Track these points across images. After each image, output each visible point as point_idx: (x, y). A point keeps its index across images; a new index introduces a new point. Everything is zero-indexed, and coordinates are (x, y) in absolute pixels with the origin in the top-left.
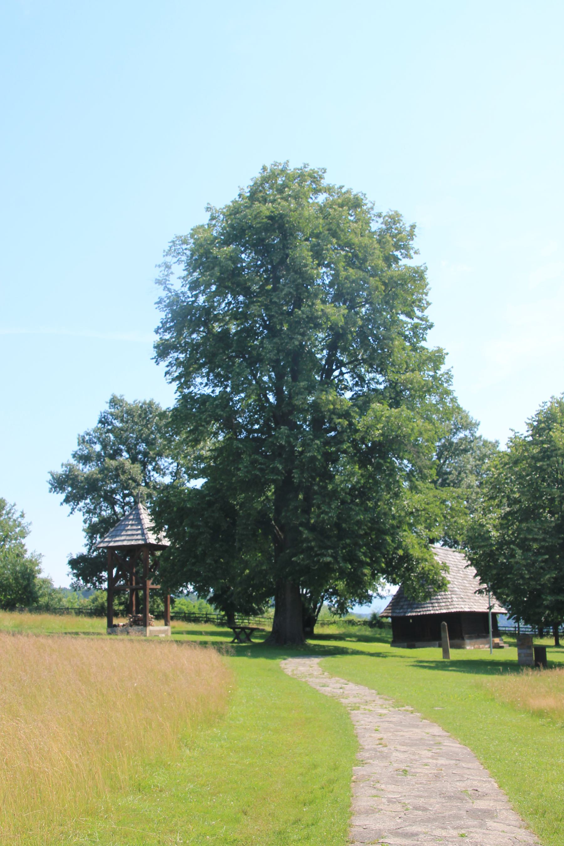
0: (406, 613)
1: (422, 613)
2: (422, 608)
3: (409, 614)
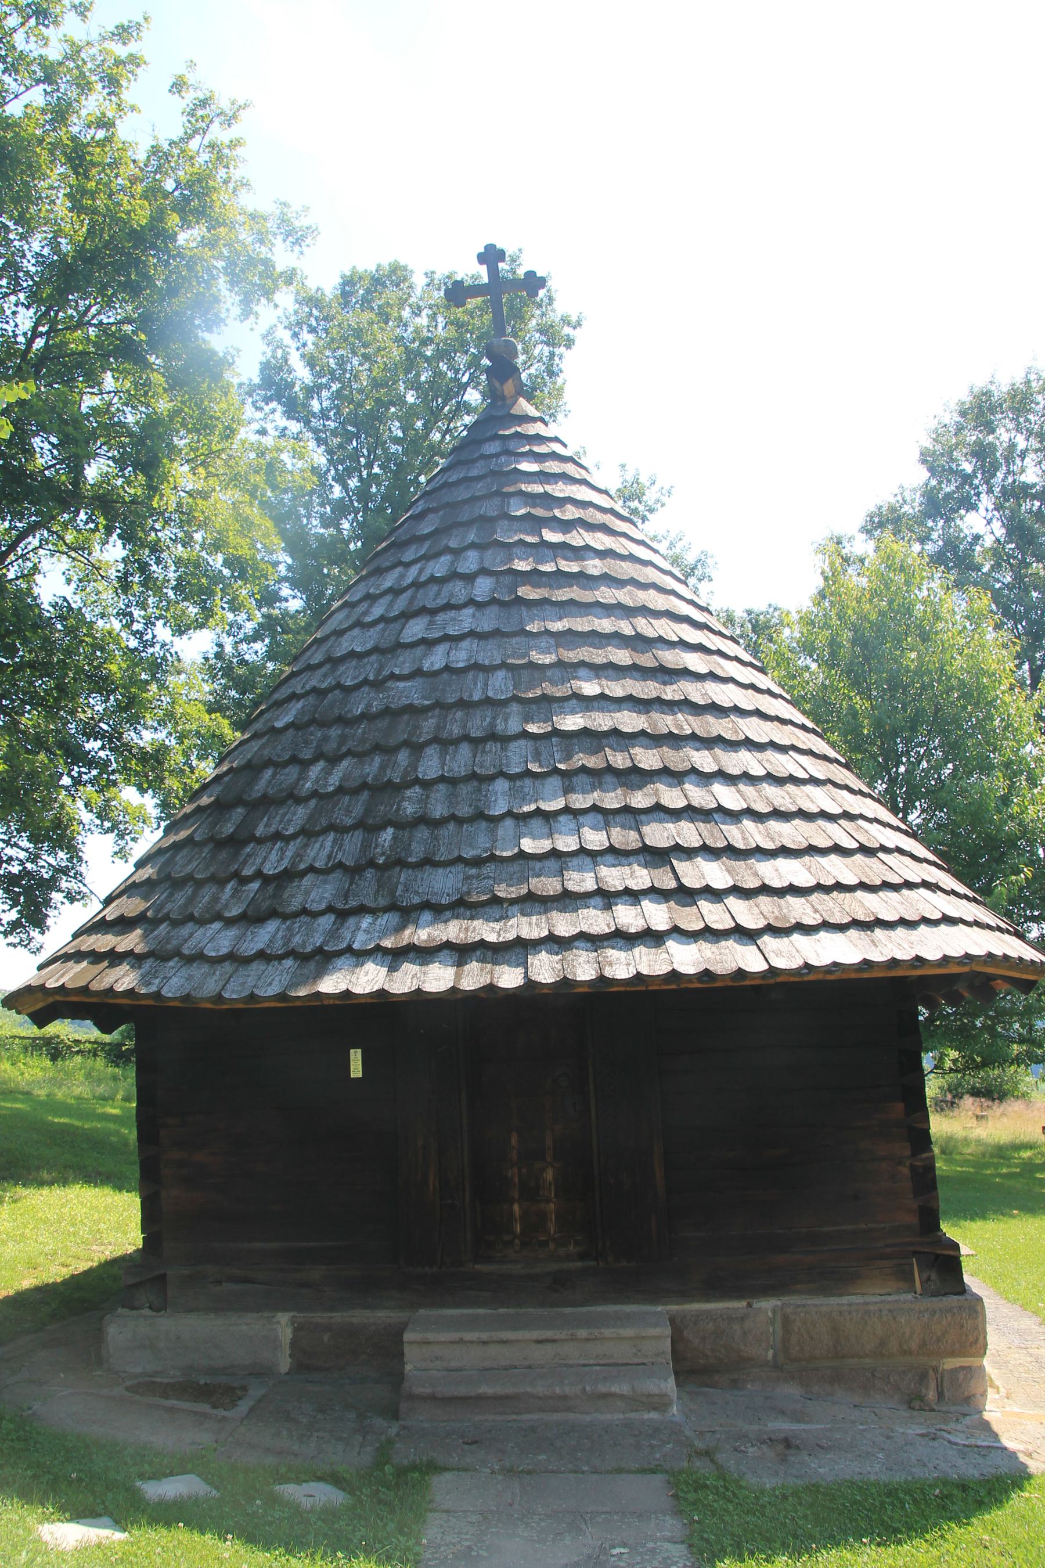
0: (323, 959)
1: (545, 969)
2: (534, 902)
3: (367, 979)
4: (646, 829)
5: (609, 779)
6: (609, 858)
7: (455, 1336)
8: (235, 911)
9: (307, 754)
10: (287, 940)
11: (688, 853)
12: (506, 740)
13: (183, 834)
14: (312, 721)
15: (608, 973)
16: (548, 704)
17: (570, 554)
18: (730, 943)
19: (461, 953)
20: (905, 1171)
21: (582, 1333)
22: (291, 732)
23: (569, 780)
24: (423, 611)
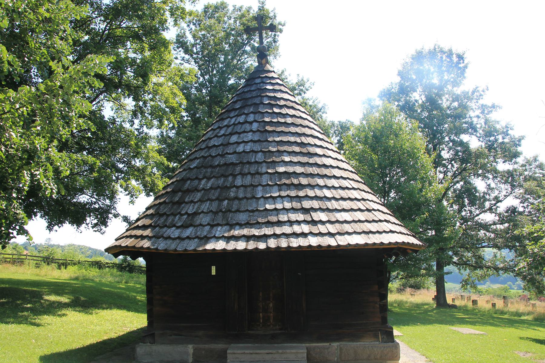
0: (206, 239)
1: (272, 243)
2: (269, 224)
3: (220, 245)
4: (303, 203)
5: (292, 187)
6: (292, 211)
7: (243, 351)
8: (179, 224)
9: (201, 177)
10: (196, 234)
11: (315, 210)
12: (261, 174)
13: (162, 200)
14: (202, 166)
15: (291, 245)
16: (274, 164)
17: (282, 116)
18: (327, 237)
19: (248, 238)
20: (378, 306)
21: (280, 351)
22: (195, 170)
23: (280, 187)
24: (236, 133)
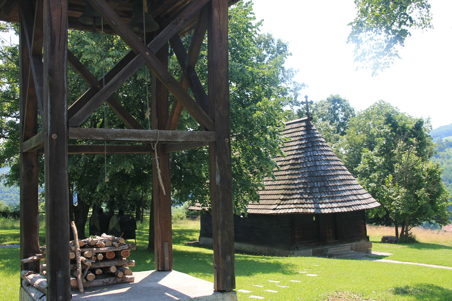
23: (344, 185)
